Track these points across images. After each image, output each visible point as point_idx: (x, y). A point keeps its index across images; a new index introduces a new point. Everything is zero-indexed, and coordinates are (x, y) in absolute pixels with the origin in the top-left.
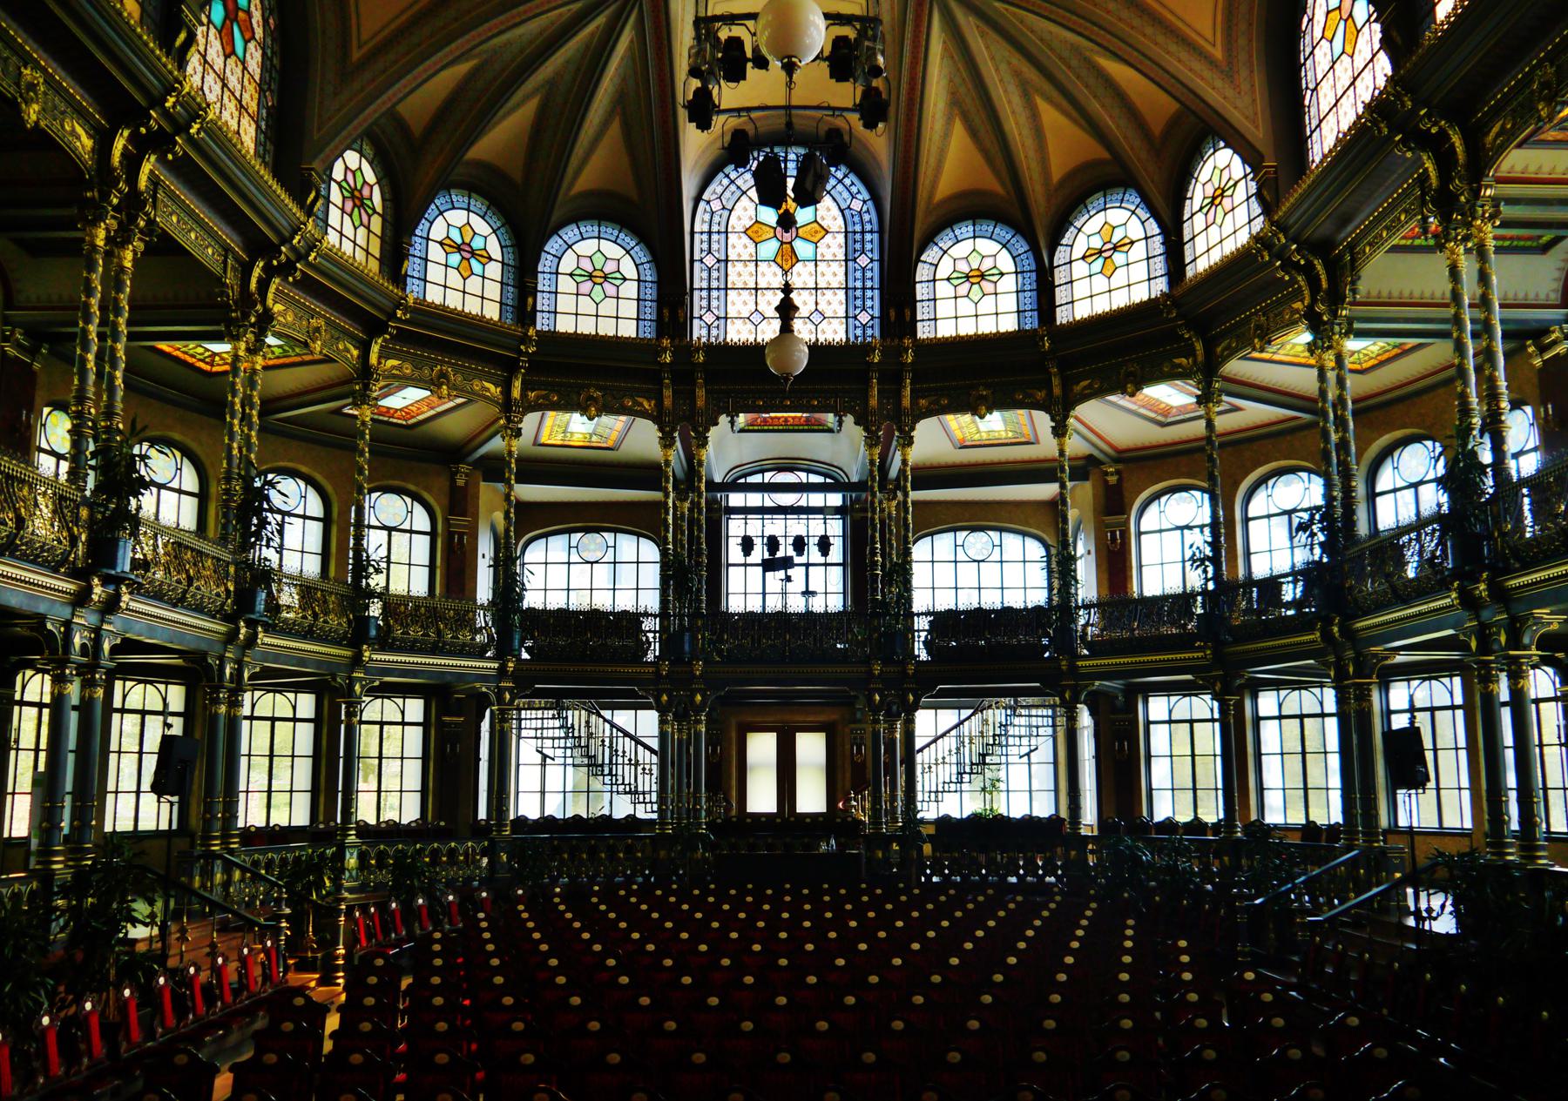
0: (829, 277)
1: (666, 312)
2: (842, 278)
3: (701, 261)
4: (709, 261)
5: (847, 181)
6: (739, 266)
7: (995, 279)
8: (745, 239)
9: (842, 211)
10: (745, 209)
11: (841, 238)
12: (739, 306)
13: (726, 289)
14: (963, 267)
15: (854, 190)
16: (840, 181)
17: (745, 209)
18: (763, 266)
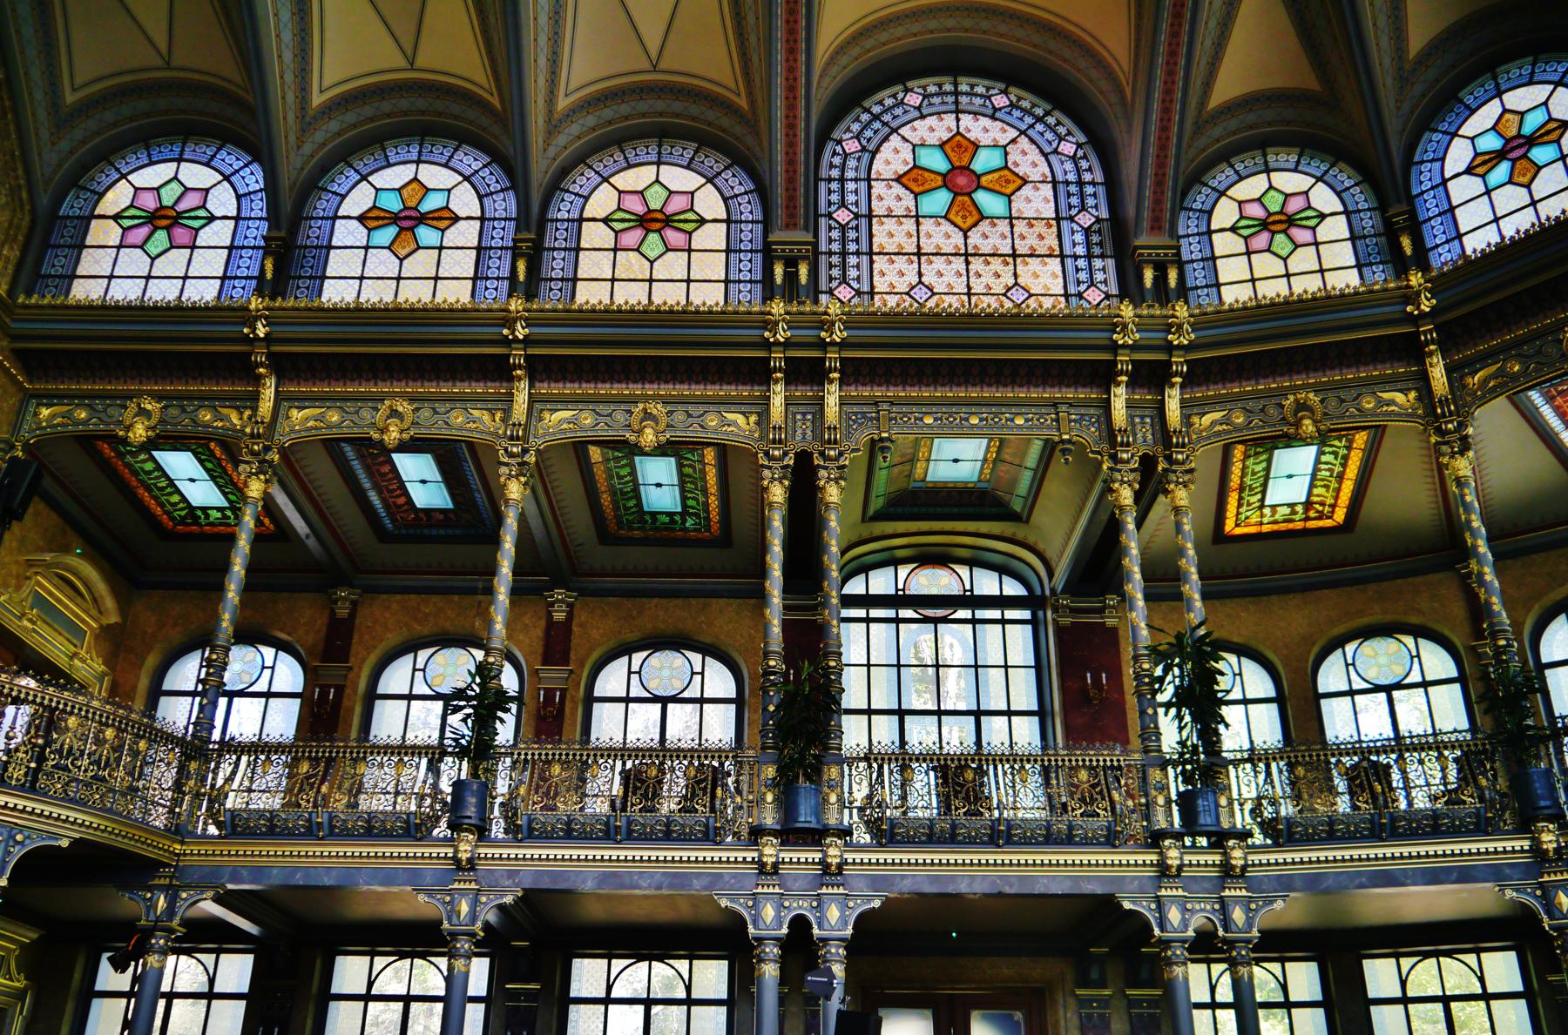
0: (1032, 241)
1: (779, 270)
2: (1055, 244)
3: (830, 216)
4: (843, 216)
5: (1051, 120)
6: (890, 224)
7: (1312, 223)
8: (898, 189)
9: (1045, 155)
10: (897, 151)
11: (1047, 190)
12: (891, 277)
13: (871, 253)
14: (1255, 211)
15: (1062, 130)
16: (1039, 119)
17: (897, 151)
18: (927, 225)
